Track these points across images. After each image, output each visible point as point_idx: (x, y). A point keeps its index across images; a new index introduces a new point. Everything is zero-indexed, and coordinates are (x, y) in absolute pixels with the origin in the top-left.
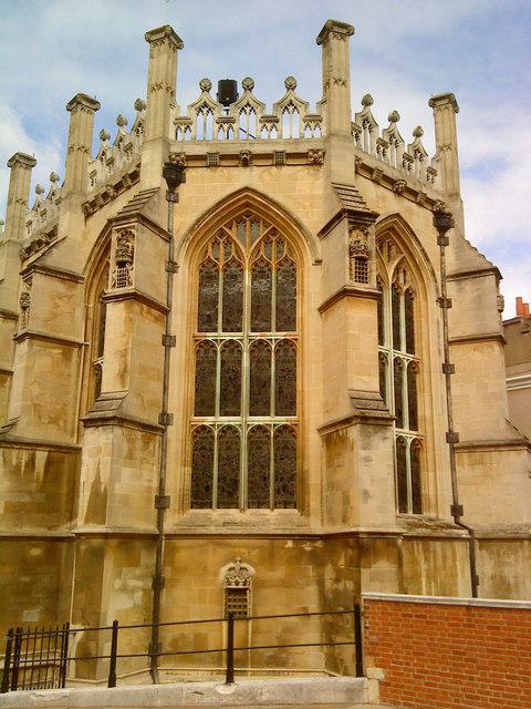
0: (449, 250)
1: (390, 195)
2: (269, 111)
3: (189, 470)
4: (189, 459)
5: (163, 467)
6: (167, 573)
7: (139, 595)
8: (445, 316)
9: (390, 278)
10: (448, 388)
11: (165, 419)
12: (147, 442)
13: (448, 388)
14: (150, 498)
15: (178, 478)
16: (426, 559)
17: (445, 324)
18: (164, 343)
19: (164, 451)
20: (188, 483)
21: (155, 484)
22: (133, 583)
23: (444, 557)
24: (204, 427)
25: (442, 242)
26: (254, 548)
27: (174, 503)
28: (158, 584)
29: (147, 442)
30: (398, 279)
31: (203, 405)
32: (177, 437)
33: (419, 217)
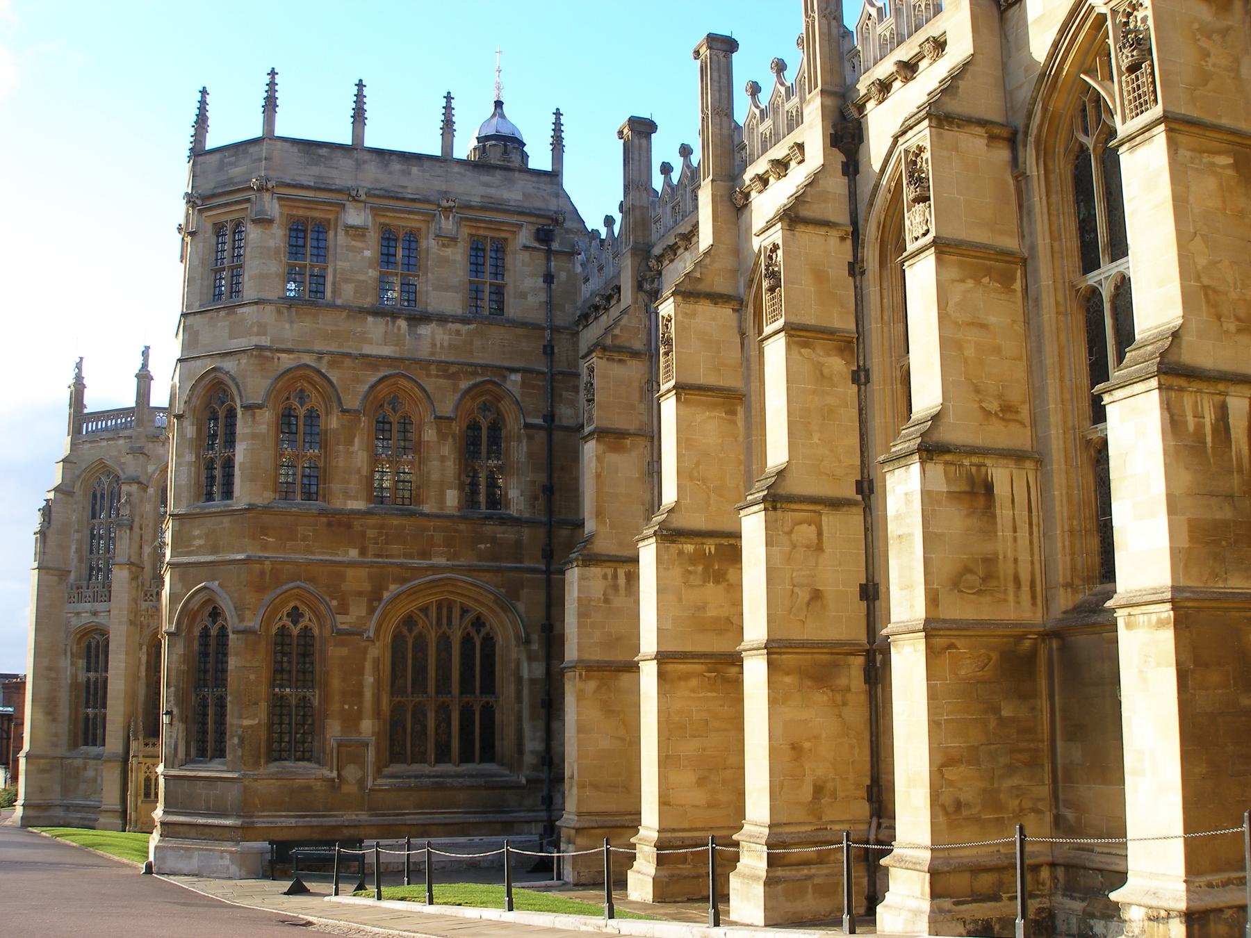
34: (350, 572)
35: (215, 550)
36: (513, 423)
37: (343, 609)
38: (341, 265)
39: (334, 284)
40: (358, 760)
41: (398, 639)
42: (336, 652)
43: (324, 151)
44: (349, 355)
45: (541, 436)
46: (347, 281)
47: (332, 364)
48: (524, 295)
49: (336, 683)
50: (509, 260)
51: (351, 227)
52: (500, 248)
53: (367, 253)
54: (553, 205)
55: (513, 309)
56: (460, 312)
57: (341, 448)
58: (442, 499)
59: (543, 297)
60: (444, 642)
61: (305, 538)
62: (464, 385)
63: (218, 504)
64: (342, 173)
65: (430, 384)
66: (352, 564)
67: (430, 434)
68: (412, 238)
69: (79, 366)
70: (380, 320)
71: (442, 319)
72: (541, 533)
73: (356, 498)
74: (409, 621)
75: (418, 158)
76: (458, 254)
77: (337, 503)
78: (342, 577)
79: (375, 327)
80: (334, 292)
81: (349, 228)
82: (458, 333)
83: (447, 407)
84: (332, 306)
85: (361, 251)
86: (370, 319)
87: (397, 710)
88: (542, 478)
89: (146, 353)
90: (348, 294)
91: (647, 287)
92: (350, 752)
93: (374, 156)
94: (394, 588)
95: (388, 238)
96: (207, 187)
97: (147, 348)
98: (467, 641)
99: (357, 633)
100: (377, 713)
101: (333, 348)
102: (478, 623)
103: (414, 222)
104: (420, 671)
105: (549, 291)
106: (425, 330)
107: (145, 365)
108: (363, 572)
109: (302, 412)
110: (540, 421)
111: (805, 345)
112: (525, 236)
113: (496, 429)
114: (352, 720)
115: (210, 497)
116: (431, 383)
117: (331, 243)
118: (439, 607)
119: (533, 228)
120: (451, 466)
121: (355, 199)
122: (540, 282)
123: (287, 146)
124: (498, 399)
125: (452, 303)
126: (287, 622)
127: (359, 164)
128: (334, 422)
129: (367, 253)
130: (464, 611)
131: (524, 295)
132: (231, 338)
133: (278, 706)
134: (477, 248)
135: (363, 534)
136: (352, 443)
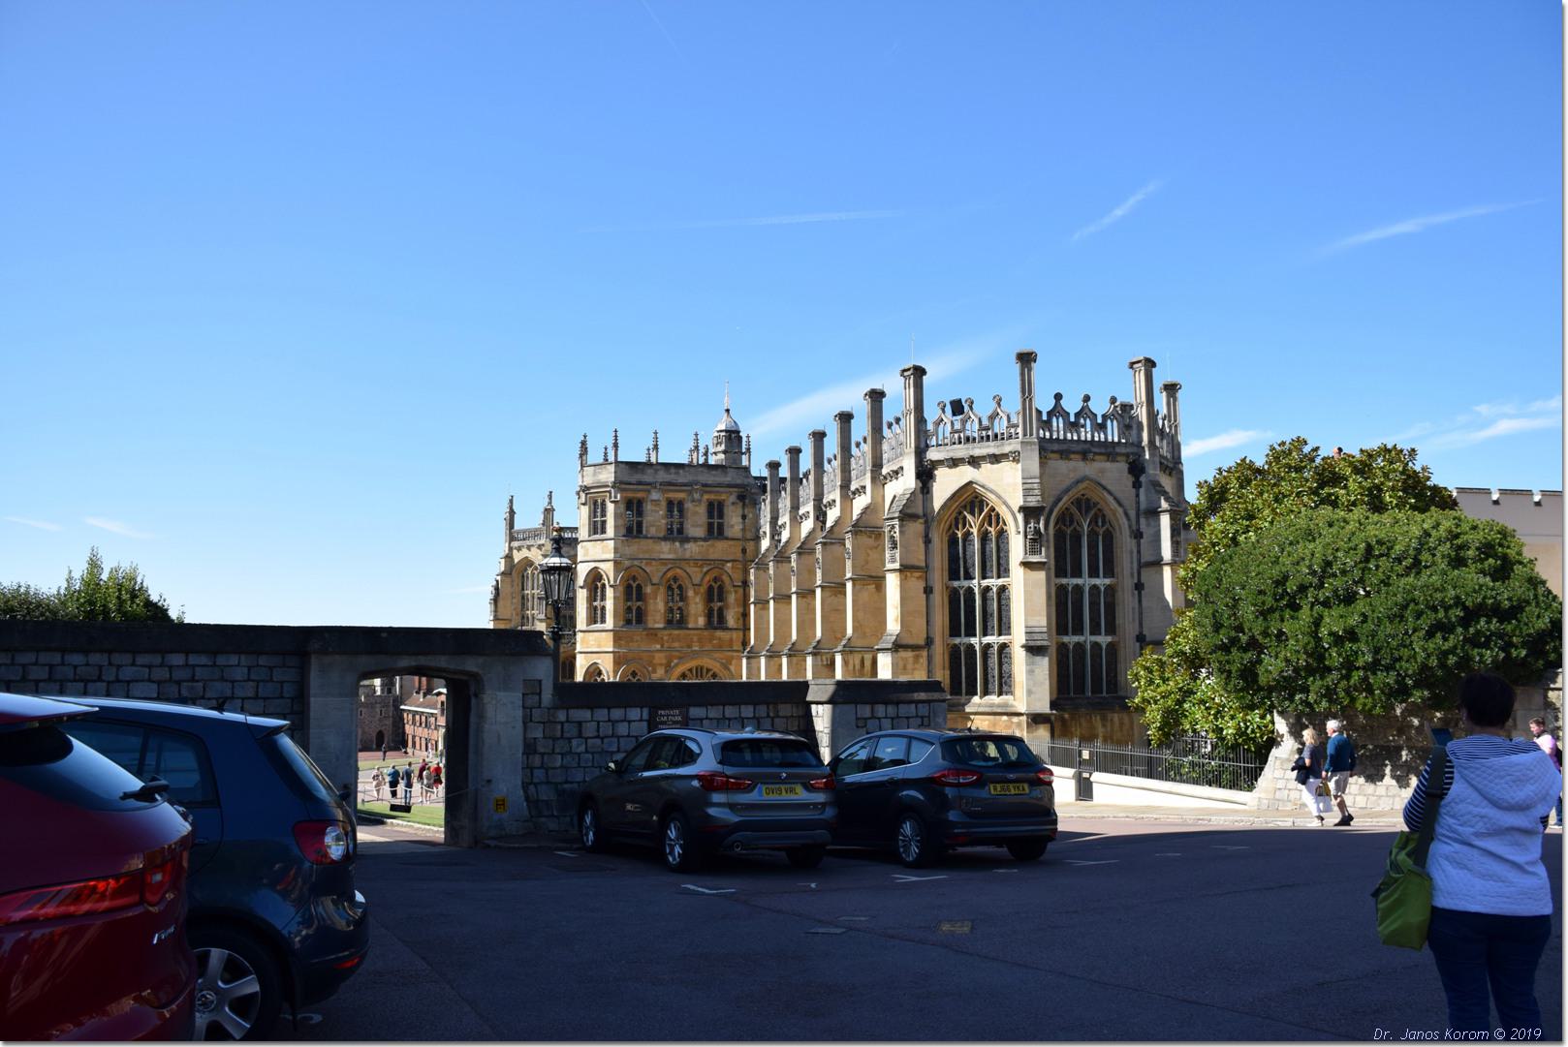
0: (1142, 491)
1: (1081, 464)
2: (985, 422)
4: (947, 665)
8: (1139, 545)
9: (1086, 528)
10: (1140, 601)
11: (929, 642)
12: (917, 658)
13: (1140, 601)
16: (1104, 726)
17: (1139, 552)
24: (955, 645)
25: (1137, 485)
26: (985, 721)
29: (917, 658)
30: (1097, 522)
31: (954, 631)
34: (657, 655)
35: (599, 646)
36: (728, 586)
37: (654, 671)
38: (649, 518)
39: (647, 527)
43: (640, 467)
44: (654, 559)
45: (741, 590)
46: (653, 526)
47: (647, 564)
48: (732, 526)
50: (725, 511)
51: (655, 501)
52: (721, 505)
53: (661, 512)
54: (746, 481)
55: (728, 533)
56: (703, 536)
57: (651, 601)
58: (696, 622)
59: (741, 527)
61: (637, 641)
62: (705, 569)
63: (598, 626)
66: (658, 651)
67: (690, 593)
68: (681, 503)
69: (511, 501)
70: (668, 543)
71: (695, 539)
72: (741, 633)
73: (658, 623)
76: (702, 510)
77: (650, 625)
78: (653, 657)
79: (665, 547)
80: (647, 531)
81: (652, 501)
82: (702, 546)
84: (646, 537)
85: (658, 512)
86: (663, 543)
88: (741, 610)
89: (550, 496)
90: (653, 531)
91: (776, 538)
93: (663, 468)
94: (676, 661)
95: (670, 503)
97: (551, 492)
101: (647, 556)
103: (681, 495)
105: (744, 523)
106: (687, 546)
107: (550, 503)
108: (662, 655)
109: (634, 585)
110: (740, 584)
111: (803, 597)
112: (733, 498)
113: (721, 588)
115: (595, 622)
116: (691, 570)
117: (644, 509)
118: (697, 669)
119: (736, 494)
121: (655, 487)
122: (741, 520)
123: (623, 466)
124: (722, 575)
126: (630, 677)
127: (656, 471)
128: (649, 590)
129: (661, 512)
130: (708, 670)
131: (732, 526)
132: (603, 553)
134: (710, 505)
135: (662, 638)
136: (656, 598)
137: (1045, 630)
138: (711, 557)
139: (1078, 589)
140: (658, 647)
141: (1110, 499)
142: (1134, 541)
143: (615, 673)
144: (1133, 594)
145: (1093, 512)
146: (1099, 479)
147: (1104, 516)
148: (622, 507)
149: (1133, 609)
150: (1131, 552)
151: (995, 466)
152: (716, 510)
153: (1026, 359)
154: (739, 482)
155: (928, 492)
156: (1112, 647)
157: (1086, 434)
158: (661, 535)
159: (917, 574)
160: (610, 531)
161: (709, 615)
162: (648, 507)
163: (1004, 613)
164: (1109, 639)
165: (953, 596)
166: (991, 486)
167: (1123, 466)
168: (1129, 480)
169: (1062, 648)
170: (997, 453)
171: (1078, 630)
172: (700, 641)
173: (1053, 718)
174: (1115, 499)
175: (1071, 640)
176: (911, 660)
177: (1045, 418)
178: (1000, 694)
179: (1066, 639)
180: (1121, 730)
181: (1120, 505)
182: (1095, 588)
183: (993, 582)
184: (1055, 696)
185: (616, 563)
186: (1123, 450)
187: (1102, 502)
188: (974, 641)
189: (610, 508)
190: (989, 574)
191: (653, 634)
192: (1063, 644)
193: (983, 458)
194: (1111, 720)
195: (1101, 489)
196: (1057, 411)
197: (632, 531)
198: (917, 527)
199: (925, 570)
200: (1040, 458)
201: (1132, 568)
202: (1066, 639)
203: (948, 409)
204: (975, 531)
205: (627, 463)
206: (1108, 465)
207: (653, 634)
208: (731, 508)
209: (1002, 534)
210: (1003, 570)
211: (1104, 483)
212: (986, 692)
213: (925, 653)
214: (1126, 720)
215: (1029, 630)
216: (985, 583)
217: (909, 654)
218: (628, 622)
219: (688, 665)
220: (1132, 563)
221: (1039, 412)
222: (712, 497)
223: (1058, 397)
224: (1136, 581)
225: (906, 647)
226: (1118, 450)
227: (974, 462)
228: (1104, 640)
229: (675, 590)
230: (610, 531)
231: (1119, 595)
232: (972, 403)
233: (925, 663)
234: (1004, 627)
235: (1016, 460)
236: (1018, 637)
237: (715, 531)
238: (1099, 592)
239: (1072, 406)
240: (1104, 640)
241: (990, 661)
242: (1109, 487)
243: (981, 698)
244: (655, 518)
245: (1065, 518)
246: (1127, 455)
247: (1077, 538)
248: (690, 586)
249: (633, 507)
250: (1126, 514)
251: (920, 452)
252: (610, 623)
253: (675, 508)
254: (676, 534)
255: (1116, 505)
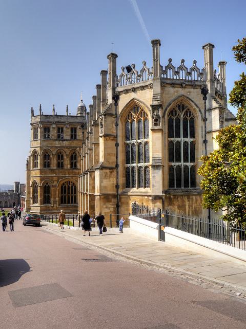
2: (139, 73)
3: (125, 178)
5: (117, 178)
6: (120, 204)
7: (112, 209)
9: (182, 117)
10: (206, 148)
11: (117, 166)
12: (111, 173)
14: (113, 187)
15: (122, 180)
16: (188, 201)
18: (116, 146)
19: (117, 174)
20: (125, 182)
21: (115, 182)
22: (109, 206)
23: (197, 200)
25: (205, 98)
27: (121, 187)
28: (118, 206)
29: (111, 173)
31: (128, 162)
32: (120, 169)
33: (194, 93)
40: (56, 204)
41: (62, 186)
42: (52, 189)
47: (51, 148)
49: (53, 193)
52: (76, 129)
55: (78, 138)
60: (69, 187)
62: (70, 150)
63: (36, 168)
64: (51, 120)
65: (65, 150)
67: (65, 157)
68: (62, 128)
71: (67, 140)
74: (64, 184)
75: (63, 116)
76: (69, 130)
79: (57, 142)
83: (68, 153)
87: (62, 196)
92: (55, 202)
94: (61, 179)
95: (59, 129)
96: (33, 122)
98: (72, 186)
99: (55, 186)
100: (59, 197)
101: (51, 146)
102: (74, 184)
103: (62, 126)
104: (65, 191)
106: (64, 142)
113: (75, 156)
114: (55, 198)
120: (69, 162)
125: (68, 138)
128: (51, 156)
130: (71, 182)
131: (79, 136)
133: (45, 197)
134: (72, 129)
136: (54, 159)
137: (161, 159)
138: (72, 146)
139: (178, 143)
140: (55, 175)
141: (193, 104)
142: (203, 122)
143: (41, 183)
144: (203, 145)
145: (185, 110)
146: (188, 96)
147: (190, 112)
148: (42, 129)
149: (203, 151)
150: (202, 127)
151: (143, 91)
152: (74, 130)
153: (156, 43)
154: (81, 121)
155: (117, 105)
156: (192, 167)
157: (182, 75)
158: (56, 139)
159: (113, 138)
160: (39, 138)
161: (72, 164)
162: (51, 130)
163: (147, 154)
164: (192, 164)
165: (127, 145)
166: (142, 100)
167: (199, 91)
168: (202, 96)
169: (171, 168)
170: (144, 85)
171: (178, 160)
172: (68, 173)
173: (164, 197)
174: (195, 104)
175: (175, 164)
176: (109, 173)
177: (164, 69)
178: (145, 187)
179: (173, 164)
180: (196, 203)
181: (197, 107)
182: (186, 143)
183: (143, 141)
184: (167, 188)
185: (41, 147)
186: (199, 84)
187: (189, 106)
188: (135, 165)
189: (39, 130)
190: (141, 137)
191: (53, 171)
192: (171, 166)
193: (137, 88)
194: (192, 199)
195: (188, 100)
196: (170, 67)
197: (46, 137)
198: (111, 120)
199: (115, 137)
200: (161, 86)
201: (202, 134)
202: (173, 164)
203: (125, 70)
204: (135, 120)
205: (46, 115)
206: (192, 90)
207: (53, 171)
208: (79, 130)
209: (146, 119)
210: (146, 136)
211: (190, 97)
212: (139, 187)
213: (115, 171)
214: (199, 198)
215: (154, 159)
216: (139, 141)
217: (108, 171)
218: (45, 166)
219: (65, 181)
220: (202, 132)
221: (161, 67)
222: (73, 126)
223: (170, 60)
224: (204, 139)
225: (106, 168)
226: (196, 83)
227: (134, 90)
228: (189, 164)
229: (60, 157)
230: (39, 138)
231: (196, 146)
232: (134, 66)
233: (115, 175)
234: (146, 159)
235: (151, 88)
236: (150, 163)
237: (74, 137)
238: (188, 144)
239: (176, 64)
240: (189, 164)
241: (141, 174)
242: (193, 99)
243: (137, 189)
244: (53, 133)
245: (173, 112)
246: (201, 86)
247: (178, 120)
248: (65, 155)
249: (46, 130)
250: (200, 111)
251: (114, 89)
252: (39, 168)
253: (60, 130)
254: (59, 138)
255: (195, 107)
